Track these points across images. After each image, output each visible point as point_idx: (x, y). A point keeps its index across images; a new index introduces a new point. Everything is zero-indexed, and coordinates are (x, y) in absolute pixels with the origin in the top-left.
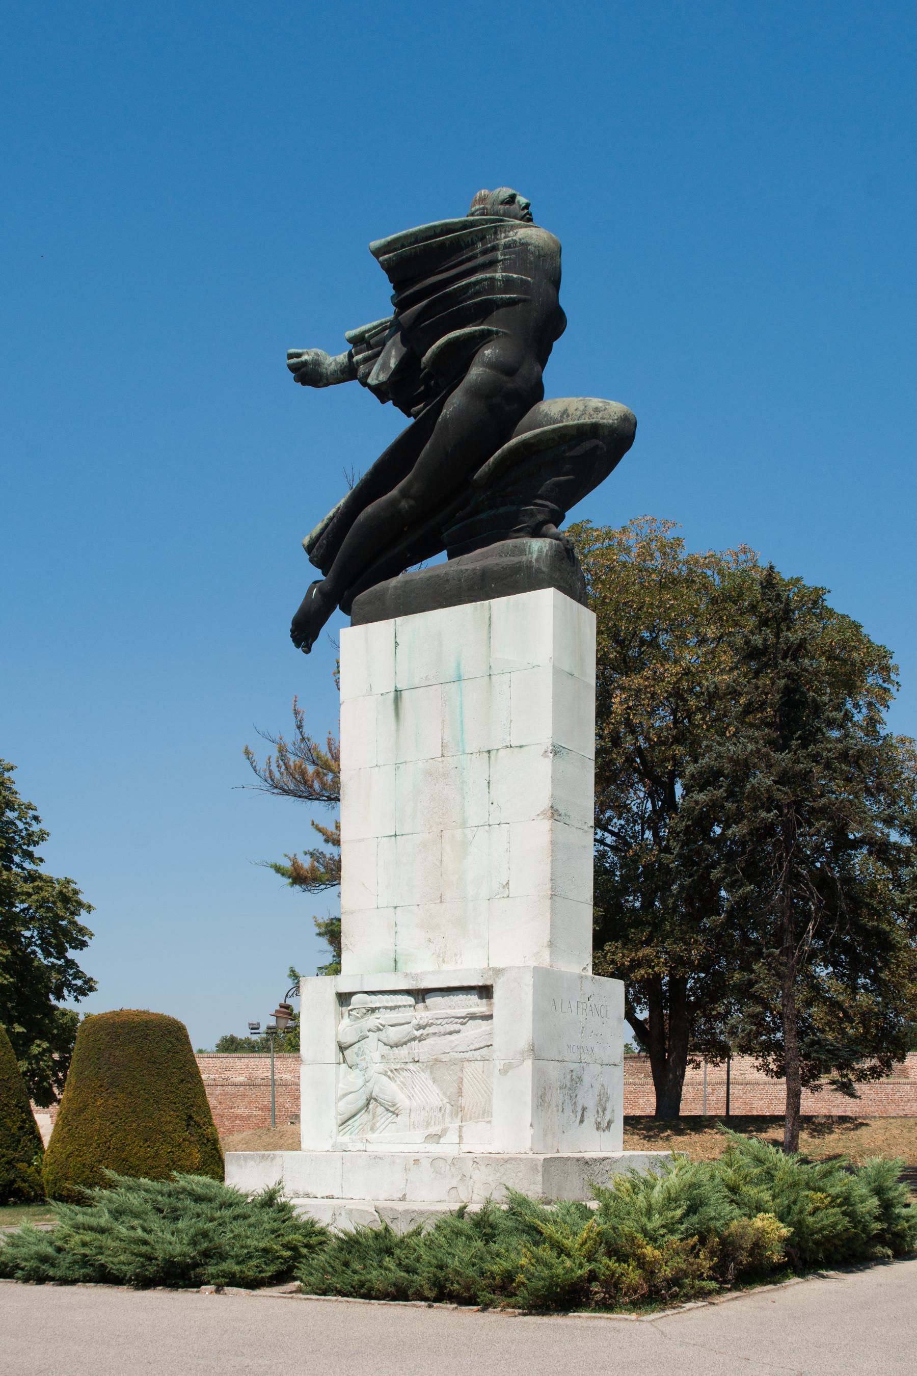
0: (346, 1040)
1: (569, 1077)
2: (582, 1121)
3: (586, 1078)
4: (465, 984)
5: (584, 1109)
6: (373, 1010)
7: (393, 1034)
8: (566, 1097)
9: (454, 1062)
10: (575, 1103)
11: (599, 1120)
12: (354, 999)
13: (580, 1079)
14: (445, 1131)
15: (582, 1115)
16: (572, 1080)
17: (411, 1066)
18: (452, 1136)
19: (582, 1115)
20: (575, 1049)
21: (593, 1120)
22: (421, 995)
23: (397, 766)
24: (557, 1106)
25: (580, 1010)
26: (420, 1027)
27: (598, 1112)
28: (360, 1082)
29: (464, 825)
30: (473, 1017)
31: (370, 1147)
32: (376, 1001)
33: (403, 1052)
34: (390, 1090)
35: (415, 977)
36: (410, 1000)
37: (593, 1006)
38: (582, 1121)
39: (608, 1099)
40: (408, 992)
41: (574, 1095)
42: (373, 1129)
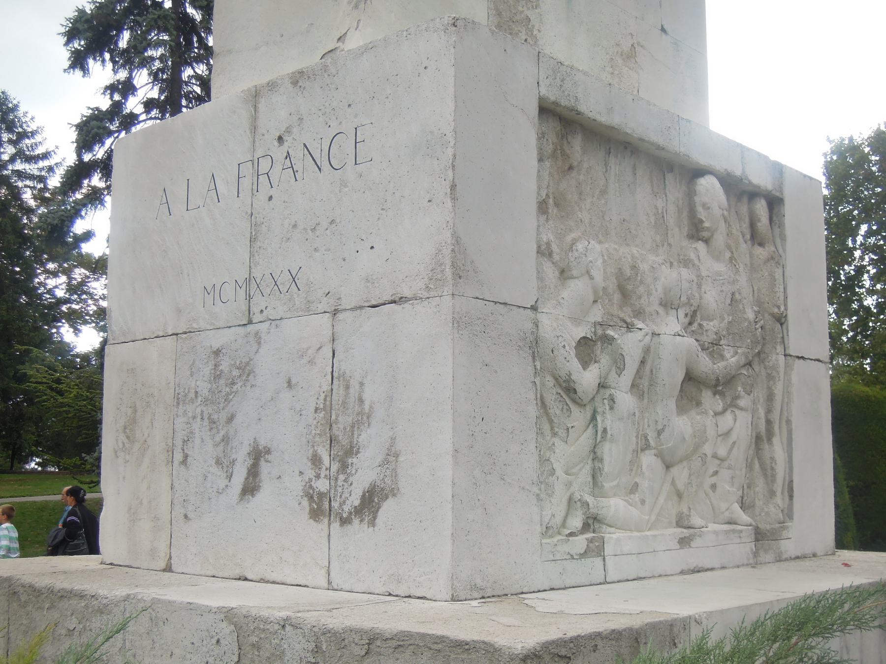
1: (207, 370)
2: (250, 489)
3: (268, 363)
5: (258, 455)
8: (197, 425)
10: (226, 440)
11: (322, 485)
13: (246, 370)
15: (253, 472)
16: (217, 376)
19: (253, 472)
20: (228, 291)
21: (296, 485)
24: (171, 450)
25: (246, 183)
27: (316, 460)
37: (298, 153)
38: (250, 489)
39: (363, 418)
41: (223, 416)
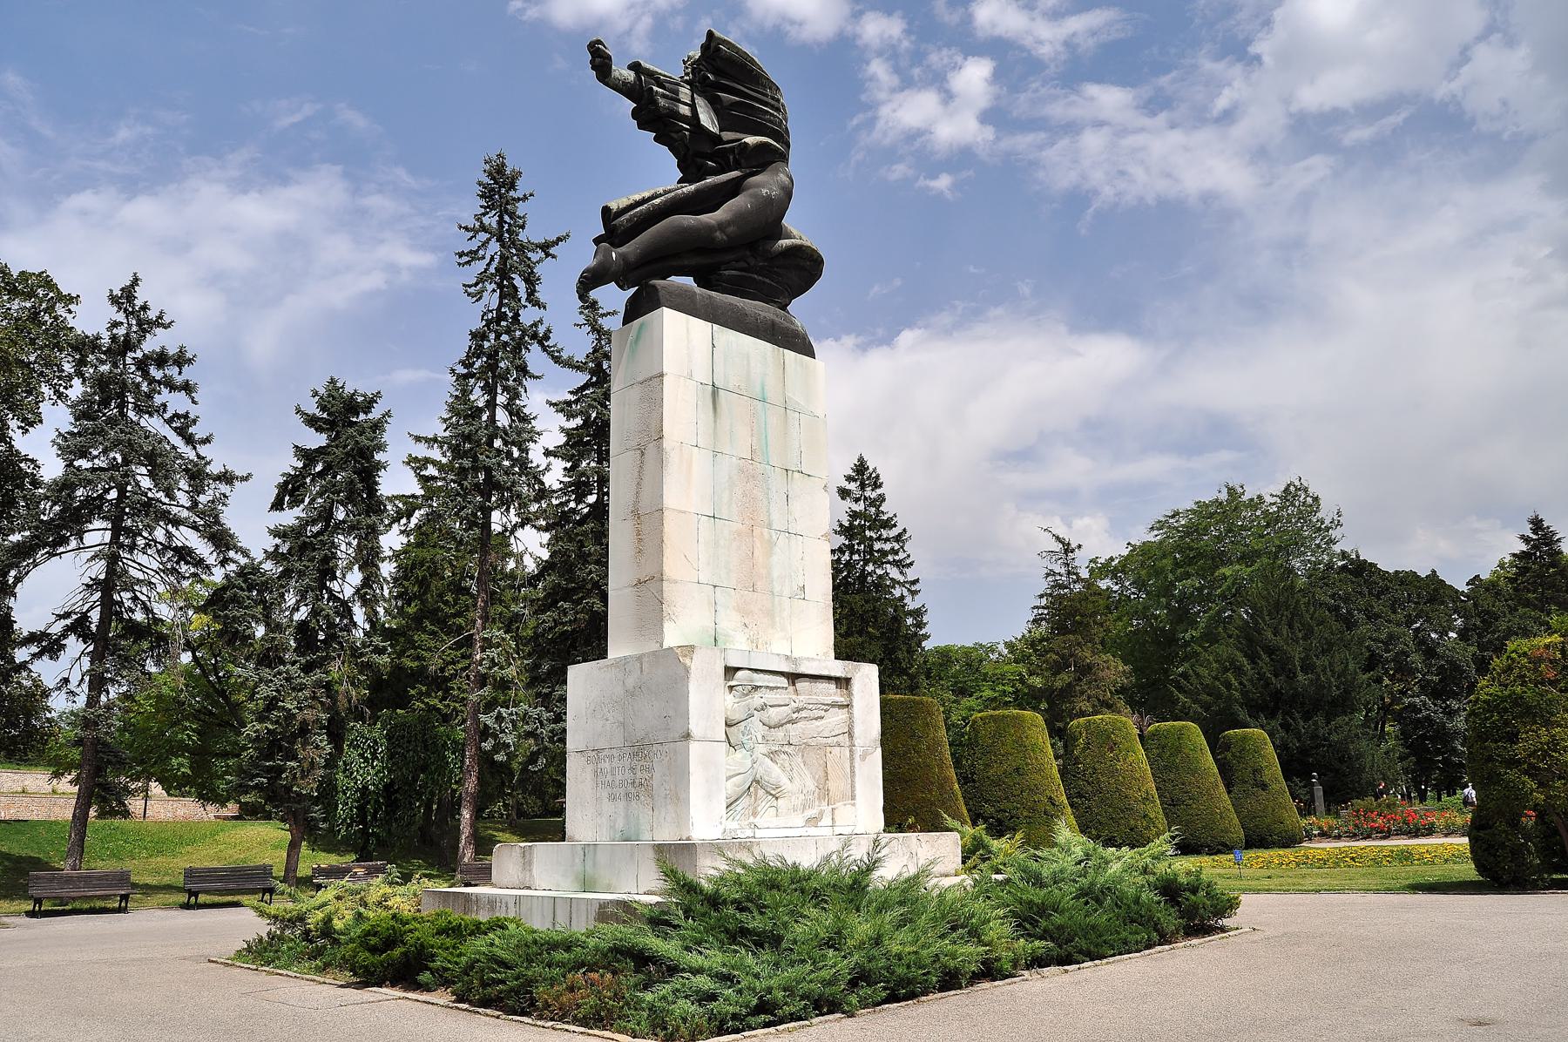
0: (737, 717)
4: (833, 674)
6: (756, 688)
7: (774, 715)
9: (820, 747)
12: (740, 673)
14: (821, 813)
17: (786, 748)
18: (827, 820)
22: (794, 677)
23: (716, 453)
26: (798, 710)
28: (749, 763)
29: (770, 527)
30: (833, 705)
31: (759, 833)
32: (761, 679)
33: (779, 734)
34: (774, 772)
35: (795, 661)
36: (783, 682)
40: (782, 674)
42: (755, 814)
